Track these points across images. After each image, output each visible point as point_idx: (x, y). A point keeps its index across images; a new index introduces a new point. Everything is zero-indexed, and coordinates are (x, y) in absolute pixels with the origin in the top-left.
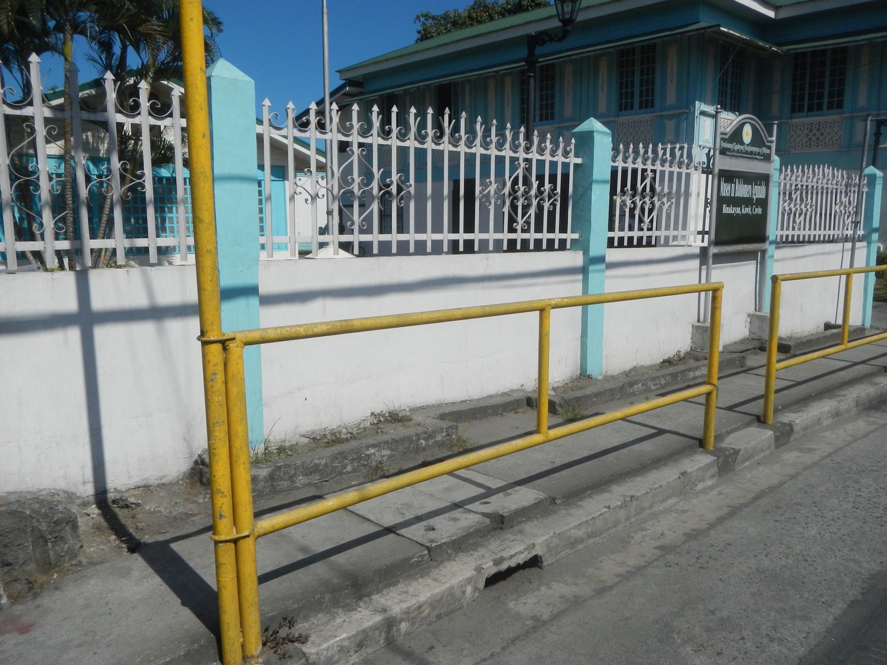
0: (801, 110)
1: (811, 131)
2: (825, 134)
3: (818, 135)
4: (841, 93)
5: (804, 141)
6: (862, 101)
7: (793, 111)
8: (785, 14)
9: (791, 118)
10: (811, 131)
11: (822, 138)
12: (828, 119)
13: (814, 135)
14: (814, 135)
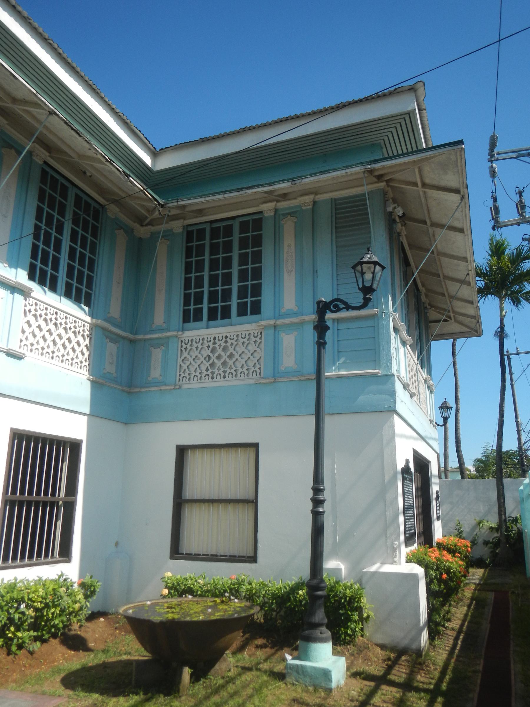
0: (198, 317)
1: (213, 351)
2: (237, 356)
3: (225, 357)
4: (257, 291)
5: (203, 369)
6: (289, 302)
7: (186, 319)
8: (166, 162)
9: (183, 330)
10: (213, 351)
11: (230, 362)
12: (237, 329)
13: (219, 357)
14: (219, 357)
